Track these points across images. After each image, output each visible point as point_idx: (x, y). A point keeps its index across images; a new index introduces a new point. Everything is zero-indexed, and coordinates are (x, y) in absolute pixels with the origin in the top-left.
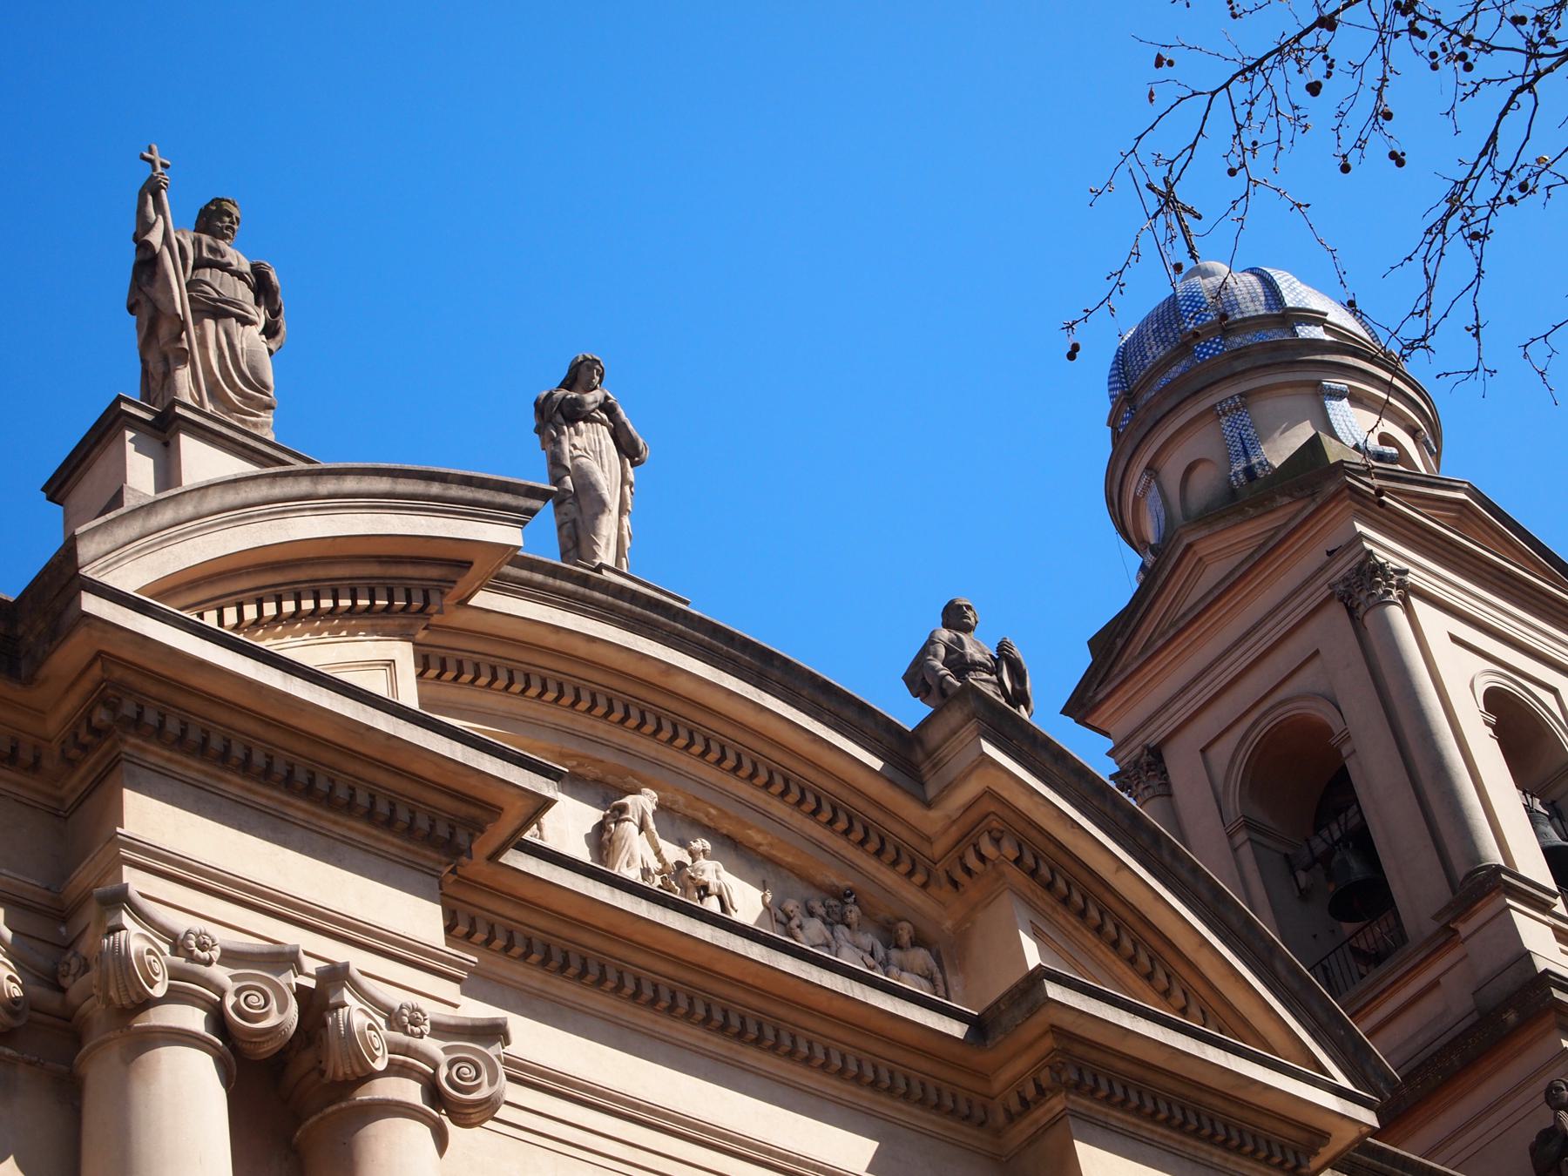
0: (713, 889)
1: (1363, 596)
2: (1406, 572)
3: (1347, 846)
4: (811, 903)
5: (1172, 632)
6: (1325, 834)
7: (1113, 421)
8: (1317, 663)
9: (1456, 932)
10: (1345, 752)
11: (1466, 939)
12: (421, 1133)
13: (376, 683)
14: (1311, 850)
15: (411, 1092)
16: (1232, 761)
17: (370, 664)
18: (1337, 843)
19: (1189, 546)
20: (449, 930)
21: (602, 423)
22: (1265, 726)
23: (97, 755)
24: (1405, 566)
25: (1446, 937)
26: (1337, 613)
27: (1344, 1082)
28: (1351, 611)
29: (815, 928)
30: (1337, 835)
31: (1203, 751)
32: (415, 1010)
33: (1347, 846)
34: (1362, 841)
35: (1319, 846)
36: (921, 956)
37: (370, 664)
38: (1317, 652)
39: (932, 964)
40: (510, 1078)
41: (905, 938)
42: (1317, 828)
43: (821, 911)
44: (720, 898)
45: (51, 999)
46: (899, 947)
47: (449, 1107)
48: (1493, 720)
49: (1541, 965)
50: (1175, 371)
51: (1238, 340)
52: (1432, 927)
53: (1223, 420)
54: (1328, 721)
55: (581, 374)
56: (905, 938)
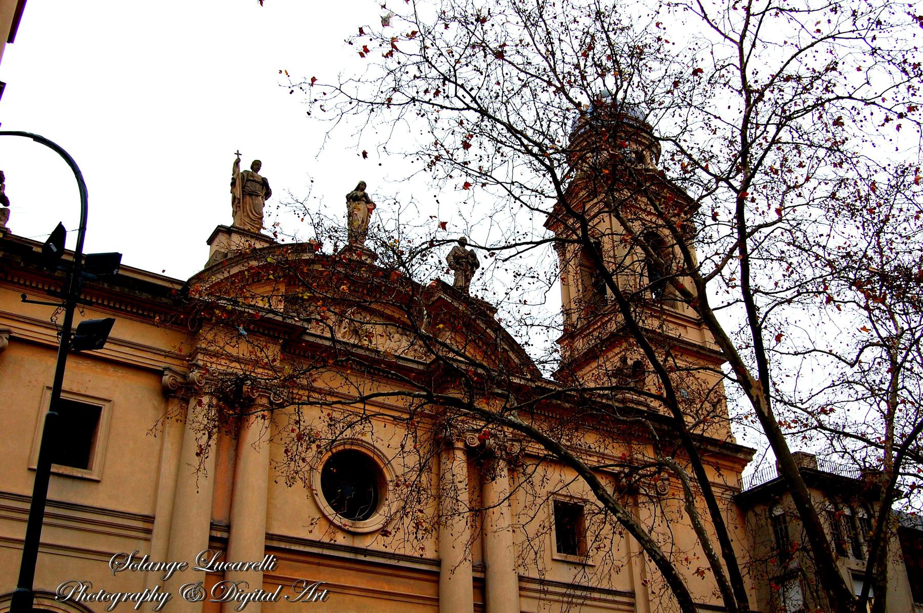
29: (397, 336)
55: (362, 186)
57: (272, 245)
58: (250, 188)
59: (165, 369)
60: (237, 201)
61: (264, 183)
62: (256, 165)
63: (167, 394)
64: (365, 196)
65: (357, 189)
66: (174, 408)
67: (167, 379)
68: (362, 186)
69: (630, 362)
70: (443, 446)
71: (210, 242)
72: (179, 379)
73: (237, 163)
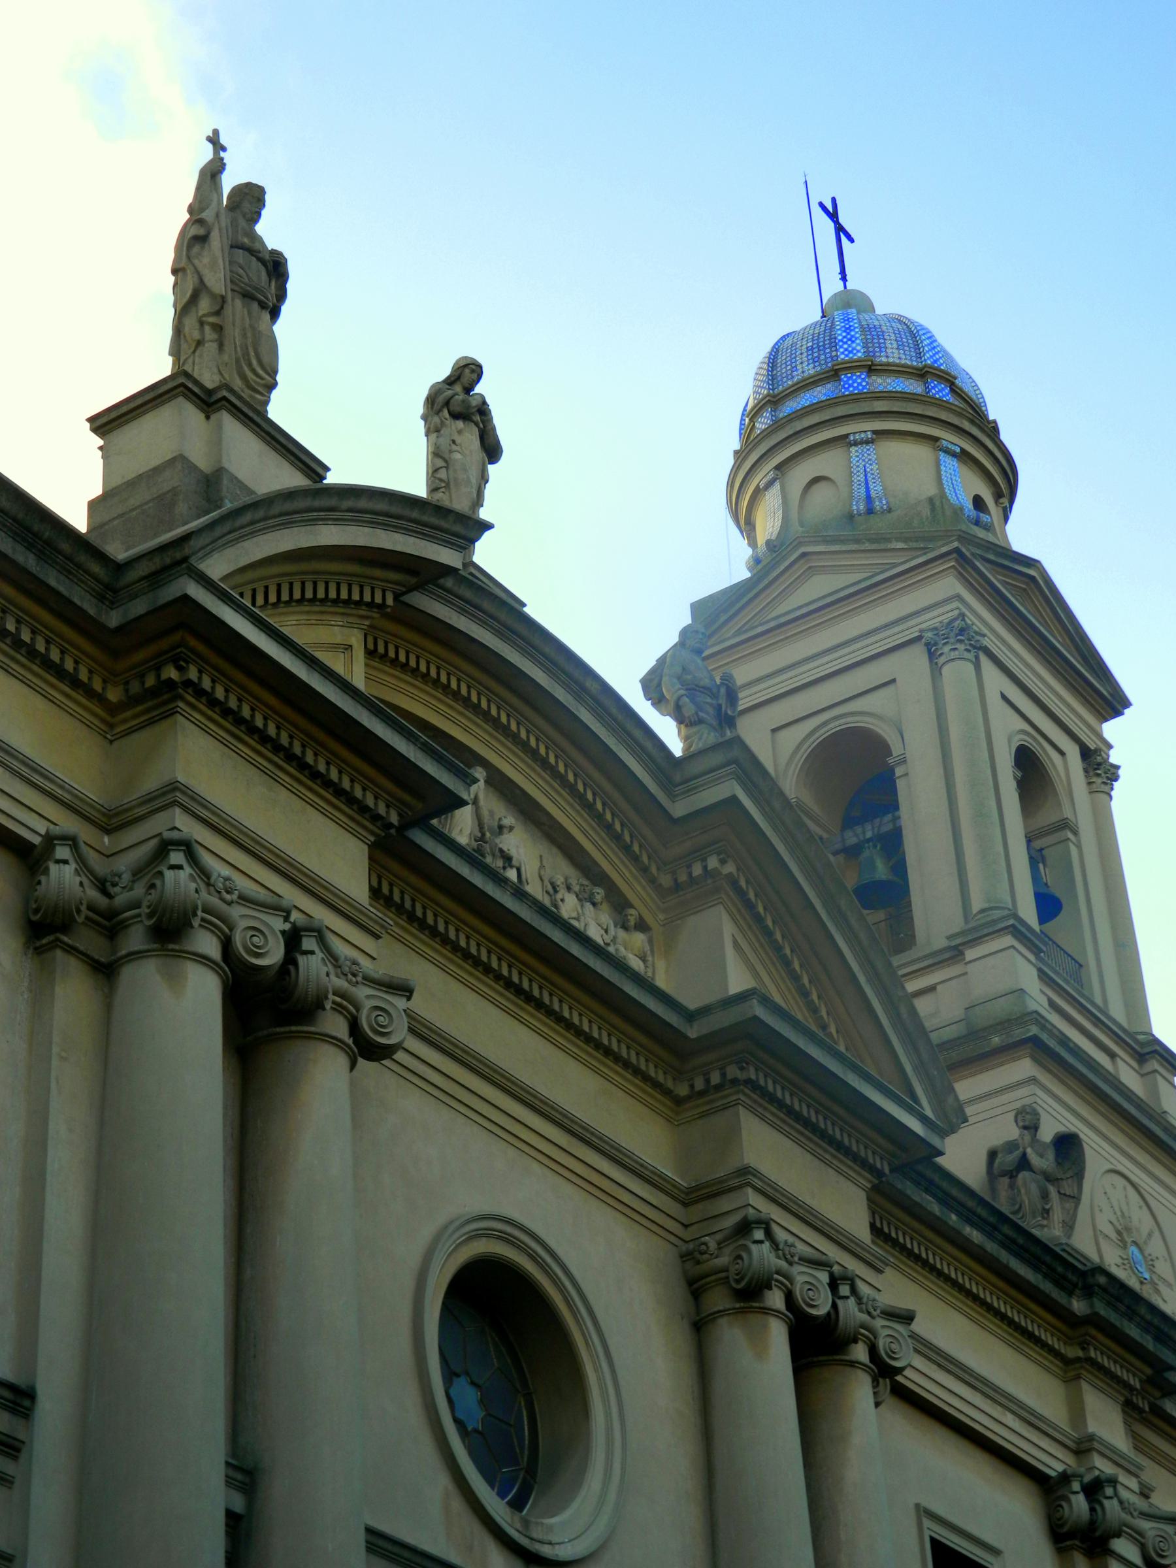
0: (514, 862)
1: (946, 649)
2: (984, 636)
3: (875, 846)
4: (570, 881)
5: (772, 624)
6: (859, 829)
7: (752, 414)
8: (890, 690)
9: (962, 953)
10: (899, 771)
11: (970, 962)
12: (342, 1060)
13: (337, 664)
14: (843, 840)
15: (338, 1027)
16: (798, 748)
17: (333, 647)
18: (869, 840)
19: (804, 555)
20: (375, 893)
21: (477, 424)
22: (835, 727)
23: (155, 702)
24: (985, 631)
25: (954, 953)
26: (919, 651)
27: (929, 1113)
28: (932, 656)
30: (869, 835)
31: (774, 731)
32: (355, 963)
33: (875, 846)
34: (892, 844)
35: (851, 839)
36: (639, 939)
37: (333, 647)
38: (894, 681)
39: (647, 948)
40: (916, 1351)
41: (632, 921)
42: (848, 822)
43: (576, 888)
44: (519, 870)
45: (101, 901)
46: (625, 928)
47: (366, 1048)
48: (1019, 774)
49: (1033, 1006)
50: (821, 393)
51: (879, 380)
52: (940, 943)
53: (853, 449)
54: (888, 739)
55: (467, 373)
56: (632, 921)
57: (313, 491)
58: (231, 274)
59: (50, 840)
60: (205, 305)
61: (276, 267)
62: (250, 199)
63: (44, 929)
64: (483, 410)
65: (450, 381)
66: (73, 991)
67: (63, 878)
68: (467, 373)
69: (1047, 1134)
70: (718, 1299)
71: (106, 423)
72: (93, 894)
73: (212, 173)
